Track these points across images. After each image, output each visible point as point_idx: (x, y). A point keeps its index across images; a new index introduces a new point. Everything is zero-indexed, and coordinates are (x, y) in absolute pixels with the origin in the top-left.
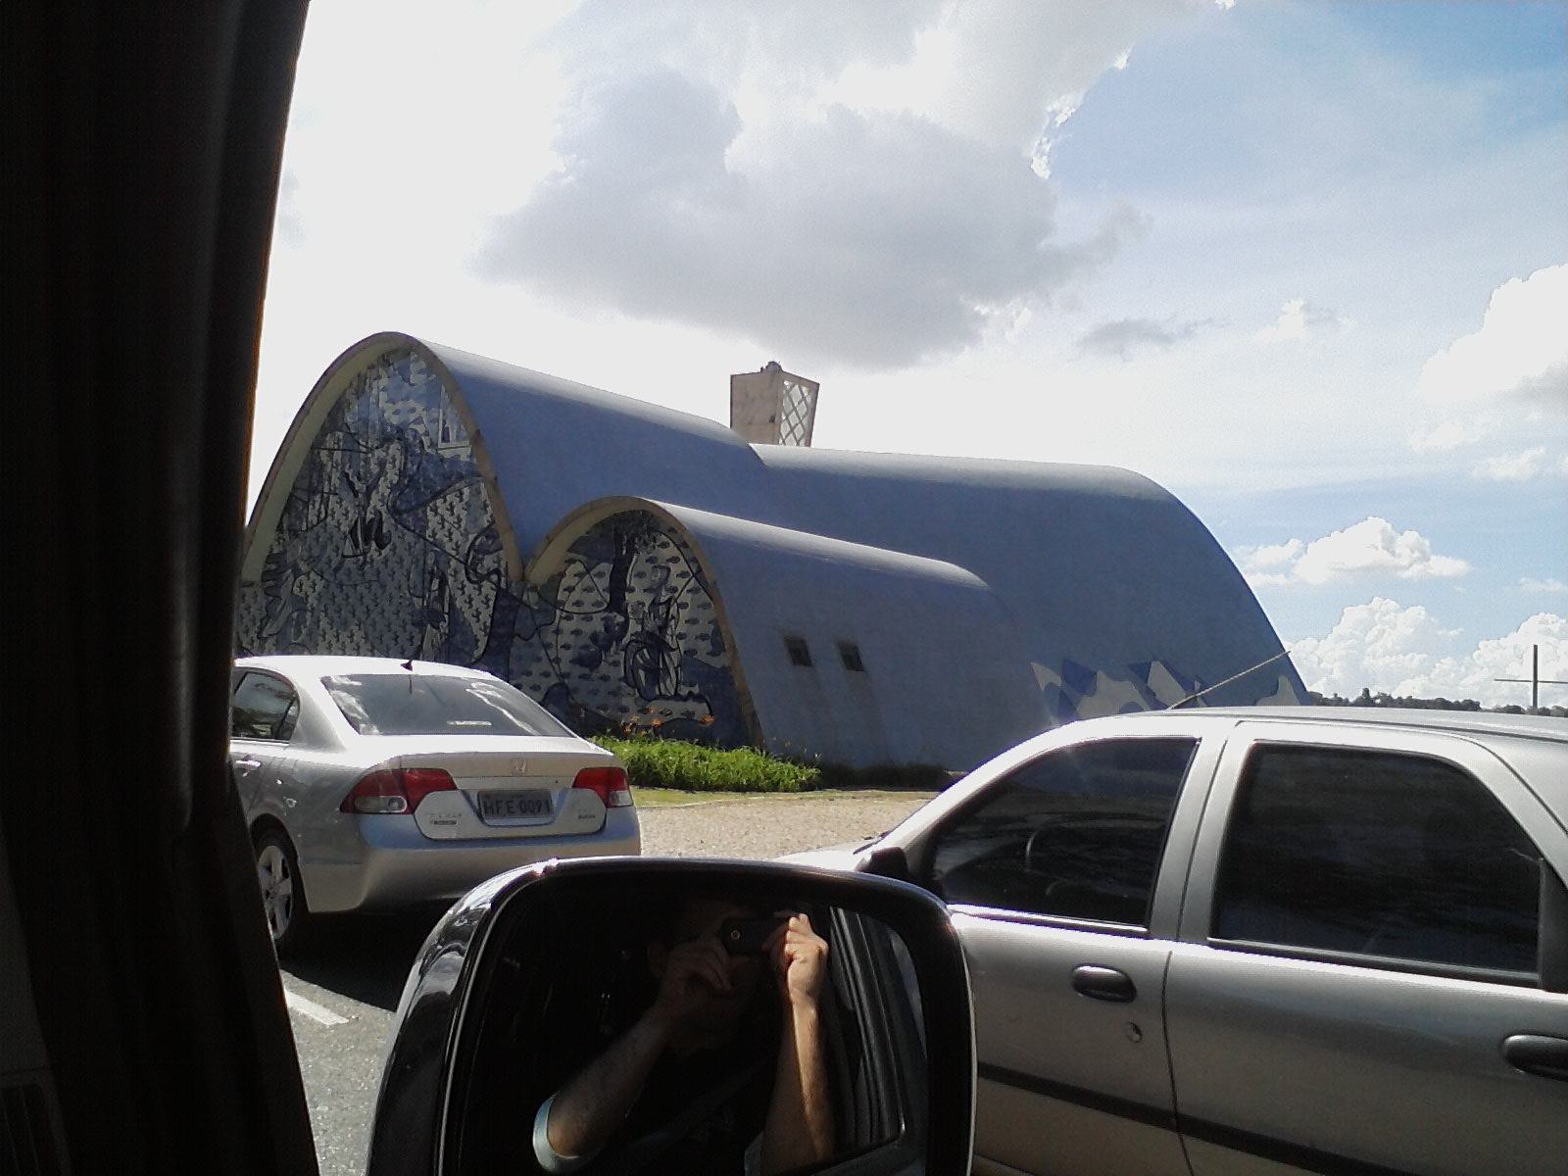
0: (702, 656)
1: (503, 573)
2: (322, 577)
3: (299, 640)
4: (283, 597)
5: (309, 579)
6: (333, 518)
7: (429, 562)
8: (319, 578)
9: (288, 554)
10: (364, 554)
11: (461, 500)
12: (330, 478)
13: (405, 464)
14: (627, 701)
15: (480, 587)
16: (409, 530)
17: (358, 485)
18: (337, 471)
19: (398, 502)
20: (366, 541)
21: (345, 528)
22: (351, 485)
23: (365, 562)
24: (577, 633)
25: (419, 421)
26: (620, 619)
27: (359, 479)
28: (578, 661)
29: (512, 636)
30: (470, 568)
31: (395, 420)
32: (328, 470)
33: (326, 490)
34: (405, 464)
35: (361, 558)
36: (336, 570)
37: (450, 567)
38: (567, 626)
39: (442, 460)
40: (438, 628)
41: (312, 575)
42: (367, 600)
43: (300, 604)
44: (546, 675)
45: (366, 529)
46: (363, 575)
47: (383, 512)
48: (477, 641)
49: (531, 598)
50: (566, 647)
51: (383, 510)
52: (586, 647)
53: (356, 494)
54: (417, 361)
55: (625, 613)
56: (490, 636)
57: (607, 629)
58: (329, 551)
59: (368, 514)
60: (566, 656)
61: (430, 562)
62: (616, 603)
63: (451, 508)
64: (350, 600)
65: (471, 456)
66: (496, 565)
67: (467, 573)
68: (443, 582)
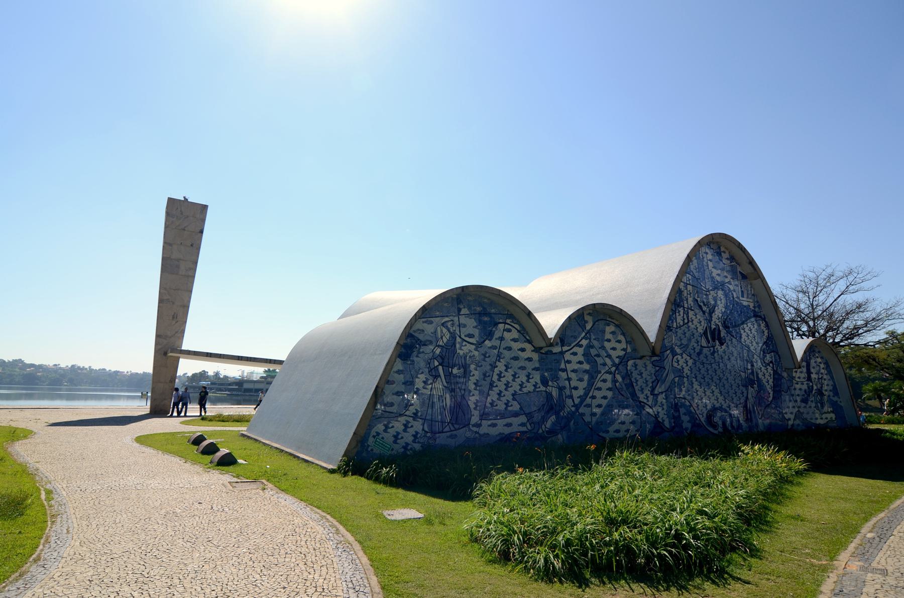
0: (832, 398)
1: (774, 363)
2: (691, 358)
3: (681, 396)
4: (667, 368)
5: (682, 358)
6: (693, 324)
7: (745, 355)
8: (689, 358)
9: (666, 341)
10: (713, 347)
11: (754, 327)
12: (687, 300)
13: (727, 304)
14: (817, 415)
15: (767, 368)
16: (733, 337)
17: (705, 308)
18: (691, 297)
19: (727, 323)
20: (714, 340)
21: (700, 330)
22: (700, 307)
23: (714, 352)
24: (800, 389)
25: (729, 283)
26: (811, 384)
27: (705, 305)
28: (803, 401)
29: (780, 391)
30: (763, 360)
31: (718, 278)
32: (685, 295)
33: (686, 306)
34: (727, 304)
35: (712, 348)
36: (699, 354)
37: (754, 358)
38: (798, 386)
39: (743, 305)
40: (753, 388)
41: (684, 355)
42: (718, 372)
43: (679, 373)
44: (794, 407)
45: (713, 333)
46: (714, 358)
47: (721, 327)
48: (769, 393)
49: (785, 375)
50: (798, 395)
51: (720, 324)
52: (803, 395)
53: (704, 312)
54: (724, 252)
55: (812, 382)
56: (774, 391)
57: (808, 387)
58: (693, 343)
59: (712, 324)
60: (799, 399)
61: (745, 355)
62: (809, 379)
63: (751, 330)
64: (709, 372)
65: (754, 307)
66: (771, 360)
67: (761, 363)
68: (752, 366)
